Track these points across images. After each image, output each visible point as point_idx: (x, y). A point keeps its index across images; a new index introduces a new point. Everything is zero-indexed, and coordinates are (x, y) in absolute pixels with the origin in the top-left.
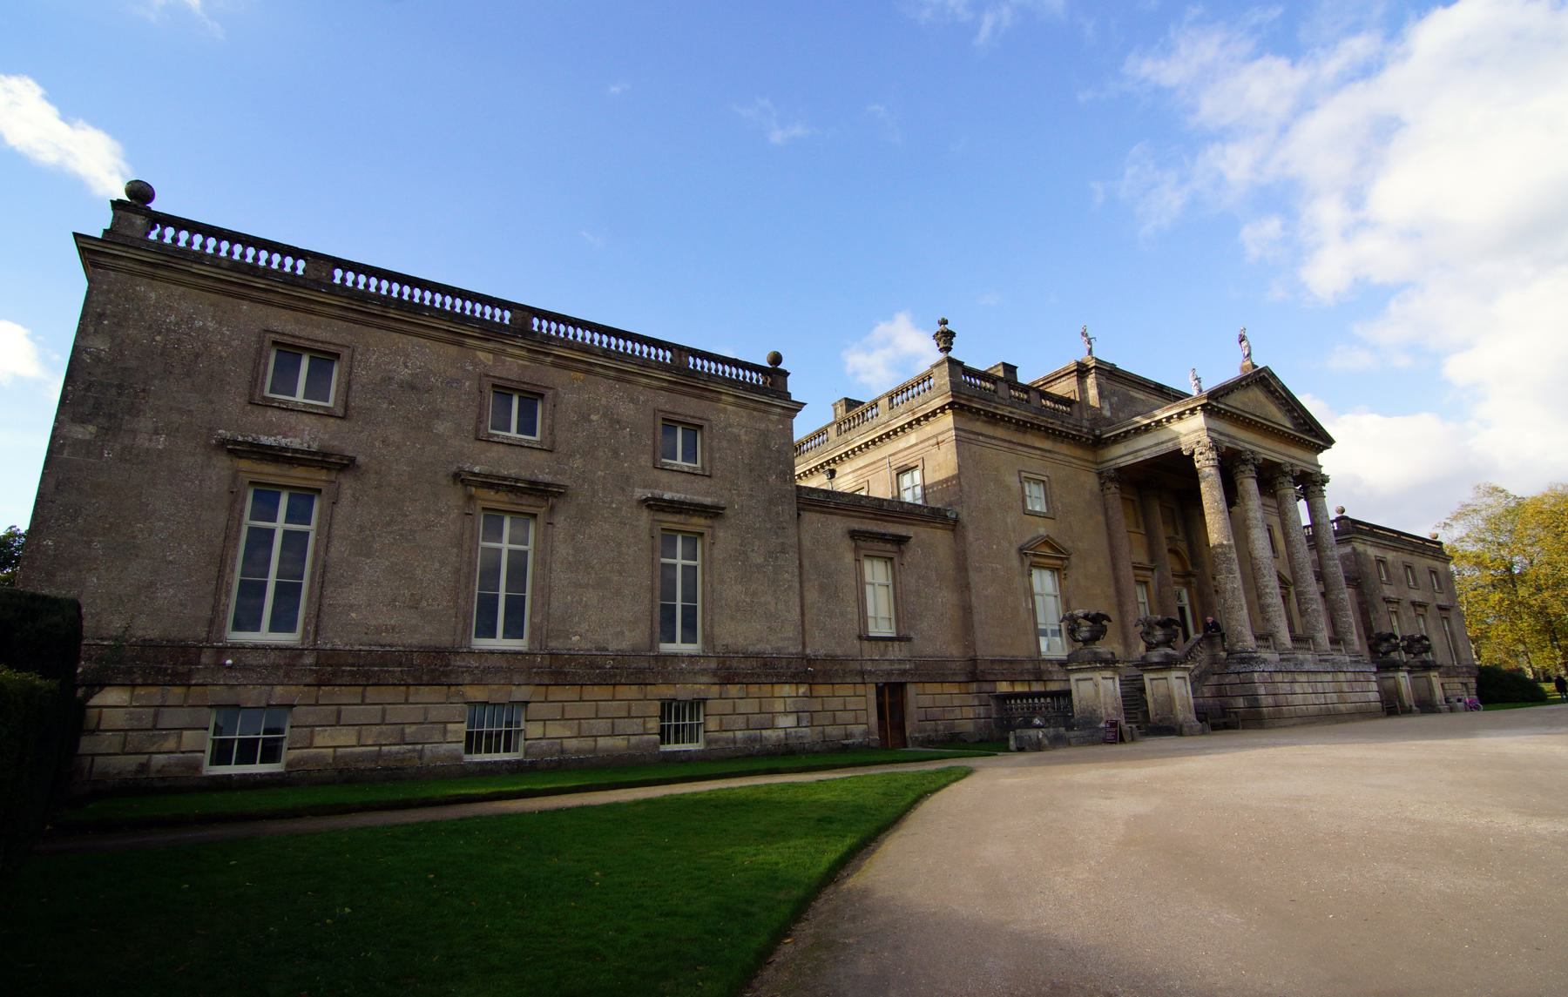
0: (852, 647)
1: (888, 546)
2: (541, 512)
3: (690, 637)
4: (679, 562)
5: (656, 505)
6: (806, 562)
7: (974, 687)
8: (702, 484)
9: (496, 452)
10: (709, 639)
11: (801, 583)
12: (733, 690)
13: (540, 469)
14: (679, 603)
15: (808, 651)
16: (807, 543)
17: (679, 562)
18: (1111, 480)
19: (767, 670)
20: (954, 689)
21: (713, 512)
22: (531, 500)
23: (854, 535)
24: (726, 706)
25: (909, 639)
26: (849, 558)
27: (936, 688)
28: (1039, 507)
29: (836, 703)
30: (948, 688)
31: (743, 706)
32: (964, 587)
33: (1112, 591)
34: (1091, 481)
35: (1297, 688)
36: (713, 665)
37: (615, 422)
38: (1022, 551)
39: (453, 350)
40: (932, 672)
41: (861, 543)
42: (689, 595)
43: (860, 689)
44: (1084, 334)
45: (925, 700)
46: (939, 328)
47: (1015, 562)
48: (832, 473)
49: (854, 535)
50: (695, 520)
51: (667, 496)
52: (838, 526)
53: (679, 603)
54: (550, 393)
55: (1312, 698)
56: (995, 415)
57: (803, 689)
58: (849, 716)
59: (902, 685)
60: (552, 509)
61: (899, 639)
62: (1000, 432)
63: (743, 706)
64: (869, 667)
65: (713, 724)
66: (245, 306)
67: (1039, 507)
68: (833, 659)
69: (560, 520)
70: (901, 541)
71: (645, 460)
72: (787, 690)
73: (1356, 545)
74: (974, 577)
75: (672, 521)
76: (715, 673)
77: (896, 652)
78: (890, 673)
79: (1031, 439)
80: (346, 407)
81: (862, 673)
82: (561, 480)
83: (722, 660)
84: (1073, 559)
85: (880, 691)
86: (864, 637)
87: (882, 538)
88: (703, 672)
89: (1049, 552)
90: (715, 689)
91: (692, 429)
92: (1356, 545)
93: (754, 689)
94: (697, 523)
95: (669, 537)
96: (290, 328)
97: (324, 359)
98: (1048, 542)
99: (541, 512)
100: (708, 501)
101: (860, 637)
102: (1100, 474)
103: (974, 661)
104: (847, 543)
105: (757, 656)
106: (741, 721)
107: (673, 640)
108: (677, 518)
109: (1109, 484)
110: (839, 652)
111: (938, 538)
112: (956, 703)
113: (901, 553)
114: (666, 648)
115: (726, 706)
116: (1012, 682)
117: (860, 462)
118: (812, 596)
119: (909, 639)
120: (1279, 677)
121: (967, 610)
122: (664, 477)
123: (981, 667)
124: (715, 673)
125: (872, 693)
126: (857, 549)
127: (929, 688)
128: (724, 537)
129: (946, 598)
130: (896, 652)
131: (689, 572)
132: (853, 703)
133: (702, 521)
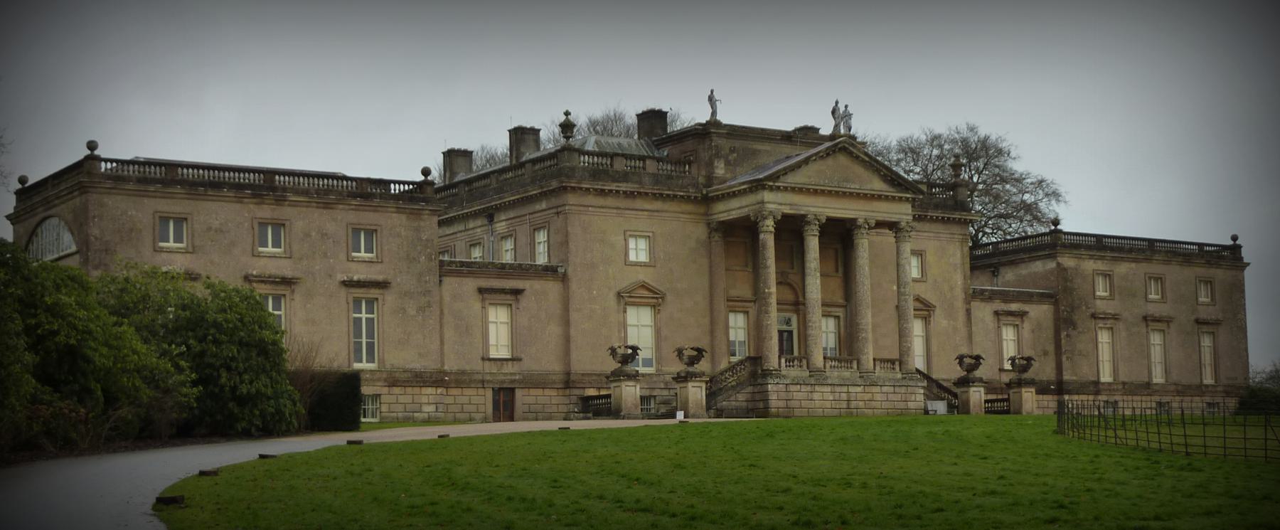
0: (478, 366)
1: (508, 297)
2: (287, 293)
3: (371, 359)
4: (364, 316)
5: (349, 284)
6: (446, 311)
7: (568, 392)
8: (379, 267)
9: (263, 261)
10: (382, 361)
11: (441, 326)
12: (397, 390)
13: (285, 268)
14: (364, 340)
15: (446, 368)
16: (447, 298)
17: (364, 316)
18: (716, 230)
19: (420, 379)
20: (553, 393)
21: (383, 285)
22: (283, 287)
23: (481, 291)
24: (392, 399)
25: (520, 360)
26: (478, 305)
27: (540, 392)
28: (643, 257)
29: (465, 400)
30: (547, 392)
31: (402, 399)
32: (566, 323)
33: (707, 321)
34: (700, 231)
35: (816, 396)
36: (385, 376)
37: (324, 235)
38: (619, 295)
39: (238, 206)
40: (536, 382)
41: (486, 296)
42: (370, 334)
43: (481, 391)
44: (711, 99)
45: (531, 400)
46: (563, 118)
47: (612, 301)
48: (491, 218)
49: (481, 291)
50: (373, 291)
51: (355, 278)
52: (470, 285)
53: (364, 340)
54: (287, 223)
55: (885, 405)
56: (603, 190)
57: (439, 390)
58: (473, 408)
59: (512, 390)
60: (293, 291)
61: (512, 360)
62: (610, 201)
63: (402, 399)
64: (488, 378)
65: (384, 408)
66: (146, 200)
67: (643, 257)
68: (463, 373)
69: (297, 297)
70: (517, 292)
71: (343, 256)
72: (430, 390)
73: (1060, 259)
74: (574, 316)
75: (359, 293)
76: (385, 380)
77: (509, 368)
78: (503, 382)
79: (639, 203)
80: (194, 247)
81: (483, 382)
82: (297, 274)
83: (391, 372)
84: (669, 298)
85: (497, 392)
86: (486, 359)
87: (503, 291)
88: (379, 380)
89: (646, 293)
90: (386, 390)
91: (370, 233)
92: (1060, 259)
93: (409, 390)
94: (374, 293)
95: (357, 302)
96: (166, 208)
97: (180, 221)
98: (644, 286)
99: (287, 293)
100: (380, 278)
101: (483, 359)
102: (708, 224)
103: (568, 374)
104: (477, 297)
105: (410, 371)
106: (401, 408)
107: (361, 361)
108: (362, 290)
109: (714, 234)
110: (468, 368)
111: (552, 288)
112: (554, 402)
113: (517, 300)
114: (357, 366)
115: (392, 399)
116: (599, 389)
117: (512, 214)
118: (449, 334)
119: (520, 360)
120: (792, 388)
121: (567, 339)
122: (353, 266)
123: (572, 378)
124: (385, 380)
125: (489, 394)
126: (483, 300)
127: (533, 392)
128: (389, 299)
129: (554, 330)
130: (509, 368)
131: (370, 322)
132: (475, 400)
133: (377, 291)
